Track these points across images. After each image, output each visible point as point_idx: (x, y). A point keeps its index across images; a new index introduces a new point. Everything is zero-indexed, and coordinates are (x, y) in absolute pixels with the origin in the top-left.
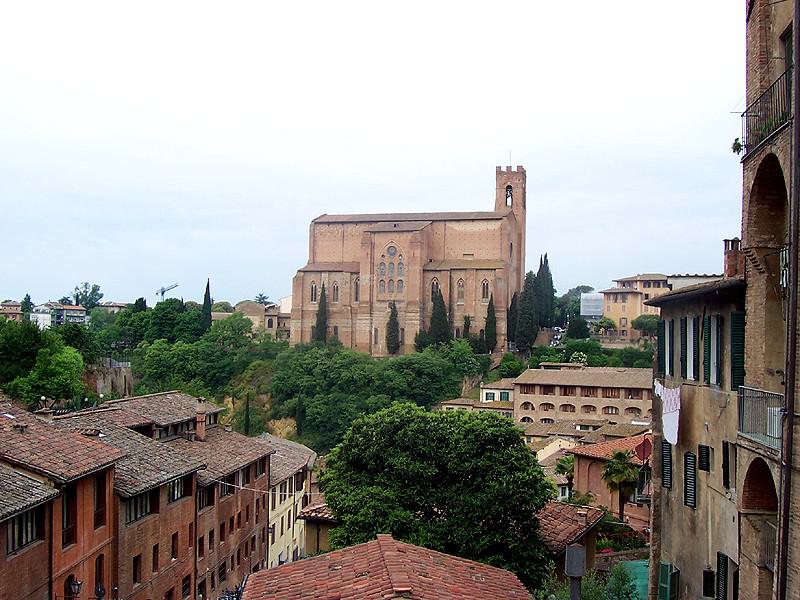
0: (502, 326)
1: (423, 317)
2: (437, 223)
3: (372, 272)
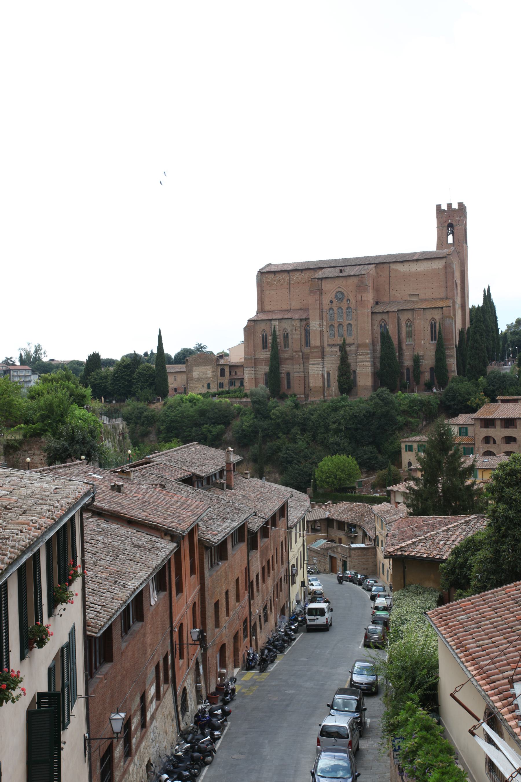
0: (452, 363)
1: (374, 358)
2: (382, 266)
3: (321, 318)
